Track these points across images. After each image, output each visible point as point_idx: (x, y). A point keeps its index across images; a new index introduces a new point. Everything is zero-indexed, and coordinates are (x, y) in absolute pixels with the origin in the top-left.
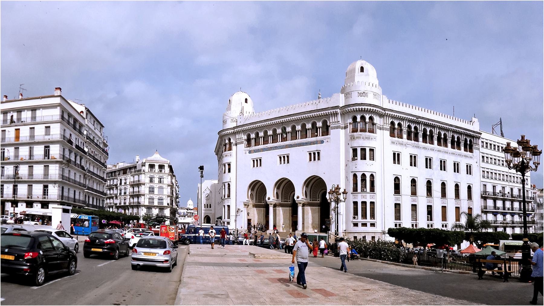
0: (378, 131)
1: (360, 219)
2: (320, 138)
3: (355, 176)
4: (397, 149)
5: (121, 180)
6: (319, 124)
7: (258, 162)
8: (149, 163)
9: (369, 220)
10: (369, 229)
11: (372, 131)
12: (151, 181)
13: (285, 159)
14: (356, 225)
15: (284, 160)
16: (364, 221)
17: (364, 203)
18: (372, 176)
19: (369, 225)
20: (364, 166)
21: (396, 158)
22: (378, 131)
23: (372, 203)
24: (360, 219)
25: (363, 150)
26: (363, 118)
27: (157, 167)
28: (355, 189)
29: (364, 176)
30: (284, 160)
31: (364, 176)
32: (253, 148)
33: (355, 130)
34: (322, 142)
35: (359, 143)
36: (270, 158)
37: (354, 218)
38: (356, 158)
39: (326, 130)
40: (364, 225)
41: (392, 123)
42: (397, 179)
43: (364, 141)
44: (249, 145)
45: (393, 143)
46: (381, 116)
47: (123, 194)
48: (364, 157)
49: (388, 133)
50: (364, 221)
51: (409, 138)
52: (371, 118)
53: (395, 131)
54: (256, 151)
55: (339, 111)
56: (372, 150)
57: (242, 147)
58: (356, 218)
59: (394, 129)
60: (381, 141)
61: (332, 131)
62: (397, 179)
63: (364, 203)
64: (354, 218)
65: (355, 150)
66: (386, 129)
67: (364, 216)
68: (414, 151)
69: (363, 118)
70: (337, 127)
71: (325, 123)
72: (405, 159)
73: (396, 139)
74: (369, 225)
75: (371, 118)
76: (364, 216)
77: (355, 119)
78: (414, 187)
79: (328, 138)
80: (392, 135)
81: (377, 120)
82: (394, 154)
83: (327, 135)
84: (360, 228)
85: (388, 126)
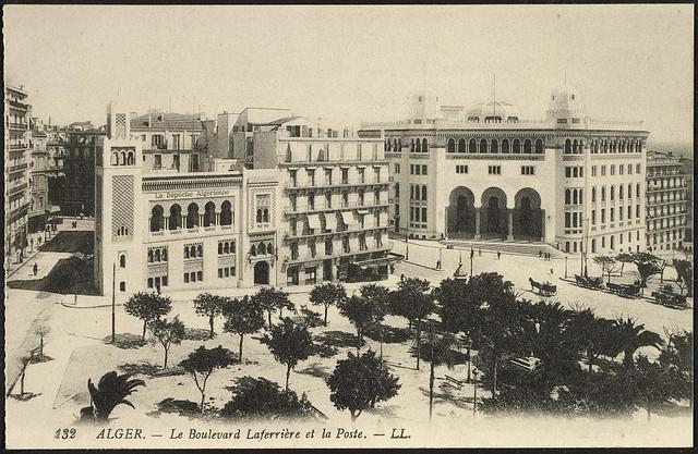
9: (579, 228)
10: (579, 235)
13: (495, 170)
17: (575, 214)
20: (575, 183)
25: (575, 169)
29: (575, 191)
31: (575, 191)
33: (568, 151)
35: (571, 164)
39: (540, 149)
40: (575, 232)
48: (575, 176)
57: (442, 152)
63: (575, 214)
70: (552, 148)
71: (539, 142)
76: (575, 226)
84: (572, 235)
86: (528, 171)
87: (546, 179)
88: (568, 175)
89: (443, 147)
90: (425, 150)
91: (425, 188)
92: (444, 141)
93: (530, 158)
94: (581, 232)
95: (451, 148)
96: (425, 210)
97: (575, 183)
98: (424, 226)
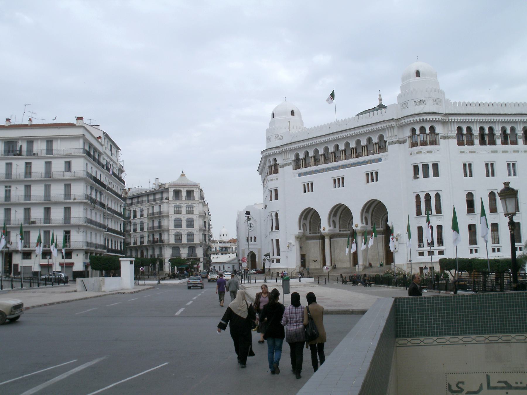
0: (442, 141)
1: (426, 248)
2: (376, 156)
3: (418, 197)
4: (467, 158)
5: (135, 211)
7: (309, 187)
8: (173, 189)
11: (434, 143)
12: (178, 212)
13: (339, 182)
14: (421, 254)
15: (339, 183)
18: (438, 196)
21: (468, 170)
22: (442, 141)
24: (426, 248)
26: (422, 129)
27: (184, 194)
29: (428, 196)
30: (339, 183)
31: (428, 196)
32: (303, 170)
34: (380, 160)
36: (323, 180)
37: (419, 246)
38: (418, 176)
39: (382, 146)
41: (459, 129)
43: (426, 155)
44: (297, 167)
45: (462, 152)
46: (444, 123)
47: (138, 230)
48: (426, 175)
49: (455, 141)
51: (483, 143)
52: (432, 129)
53: (464, 137)
54: (305, 174)
55: (393, 123)
56: (436, 166)
58: (422, 246)
59: (462, 135)
60: (448, 153)
61: (389, 147)
64: (419, 246)
65: (416, 168)
66: (452, 137)
68: (490, 158)
69: (422, 129)
70: (394, 143)
71: (381, 137)
72: (479, 169)
73: (466, 146)
75: (432, 129)
77: (413, 130)
78: (493, 202)
79: (387, 155)
80: (460, 143)
81: (439, 129)
82: (465, 165)
84: (426, 258)
85: (455, 133)
86: (373, 177)
87: (393, 180)
90: (276, 171)
91: (277, 215)
93: (373, 161)
95: (297, 163)
96: (278, 241)
97: (428, 185)
98: (278, 261)
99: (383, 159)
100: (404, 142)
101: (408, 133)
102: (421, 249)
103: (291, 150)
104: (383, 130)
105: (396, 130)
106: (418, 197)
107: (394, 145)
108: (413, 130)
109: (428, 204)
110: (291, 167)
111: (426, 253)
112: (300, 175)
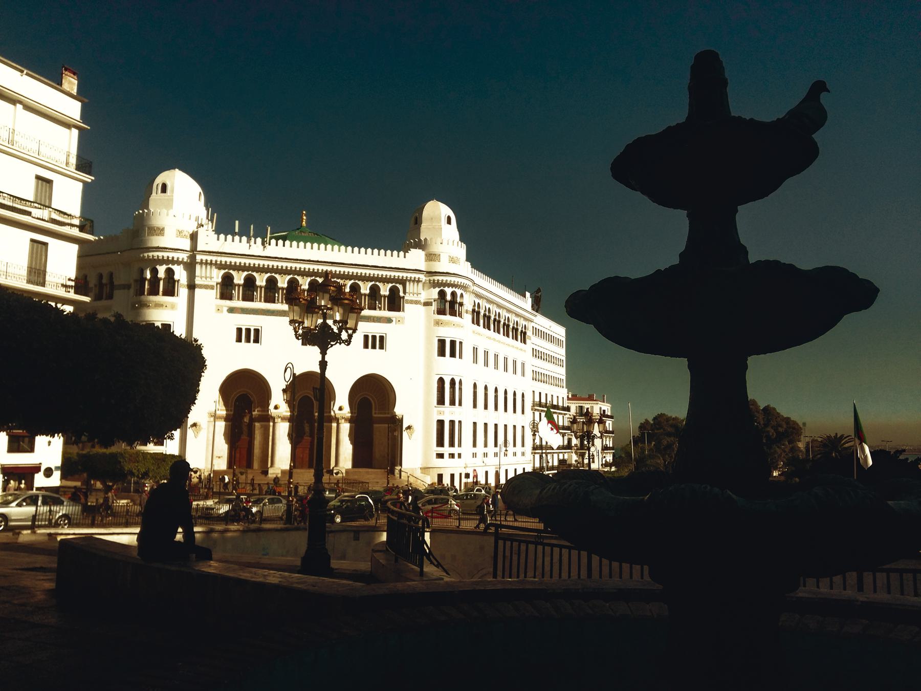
1: (446, 450)
3: (441, 381)
6: (385, 290)
9: (455, 450)
14: (441, 456)
16: (452, 450)
19: (456, 456)
23: (460, 422)
28: (441, 401)
31: (453, 382)
34: (389, 320)
35: (448, 333)
39: (395, 302)
40: (452, 456)
42: (475, 386)
50: (452, 450)
61: (406, 306)
62: (475, 386)
63: (452, 423)
65: (442, 343)
67: (452, 444)
70: (417, 302)
74: (456, 456)
76: (452, 444)
83: (399, 310)
88: (442, 353)
89: (212, 287)
92: (217, 276)
94: (460, 456)
95: (226, 289)
99: (394, 320)
100: (427, 304)
101: (434, 293)
102: (440, 450)
103: (220, 266)
104: (403, 282)
105: (420, 285)
106: (441, 381)
107: (414, 305)
108: (442, 294)
109: (446, 391)
110: (214, 294)
111: (446, 456)
112: (231, 310)
